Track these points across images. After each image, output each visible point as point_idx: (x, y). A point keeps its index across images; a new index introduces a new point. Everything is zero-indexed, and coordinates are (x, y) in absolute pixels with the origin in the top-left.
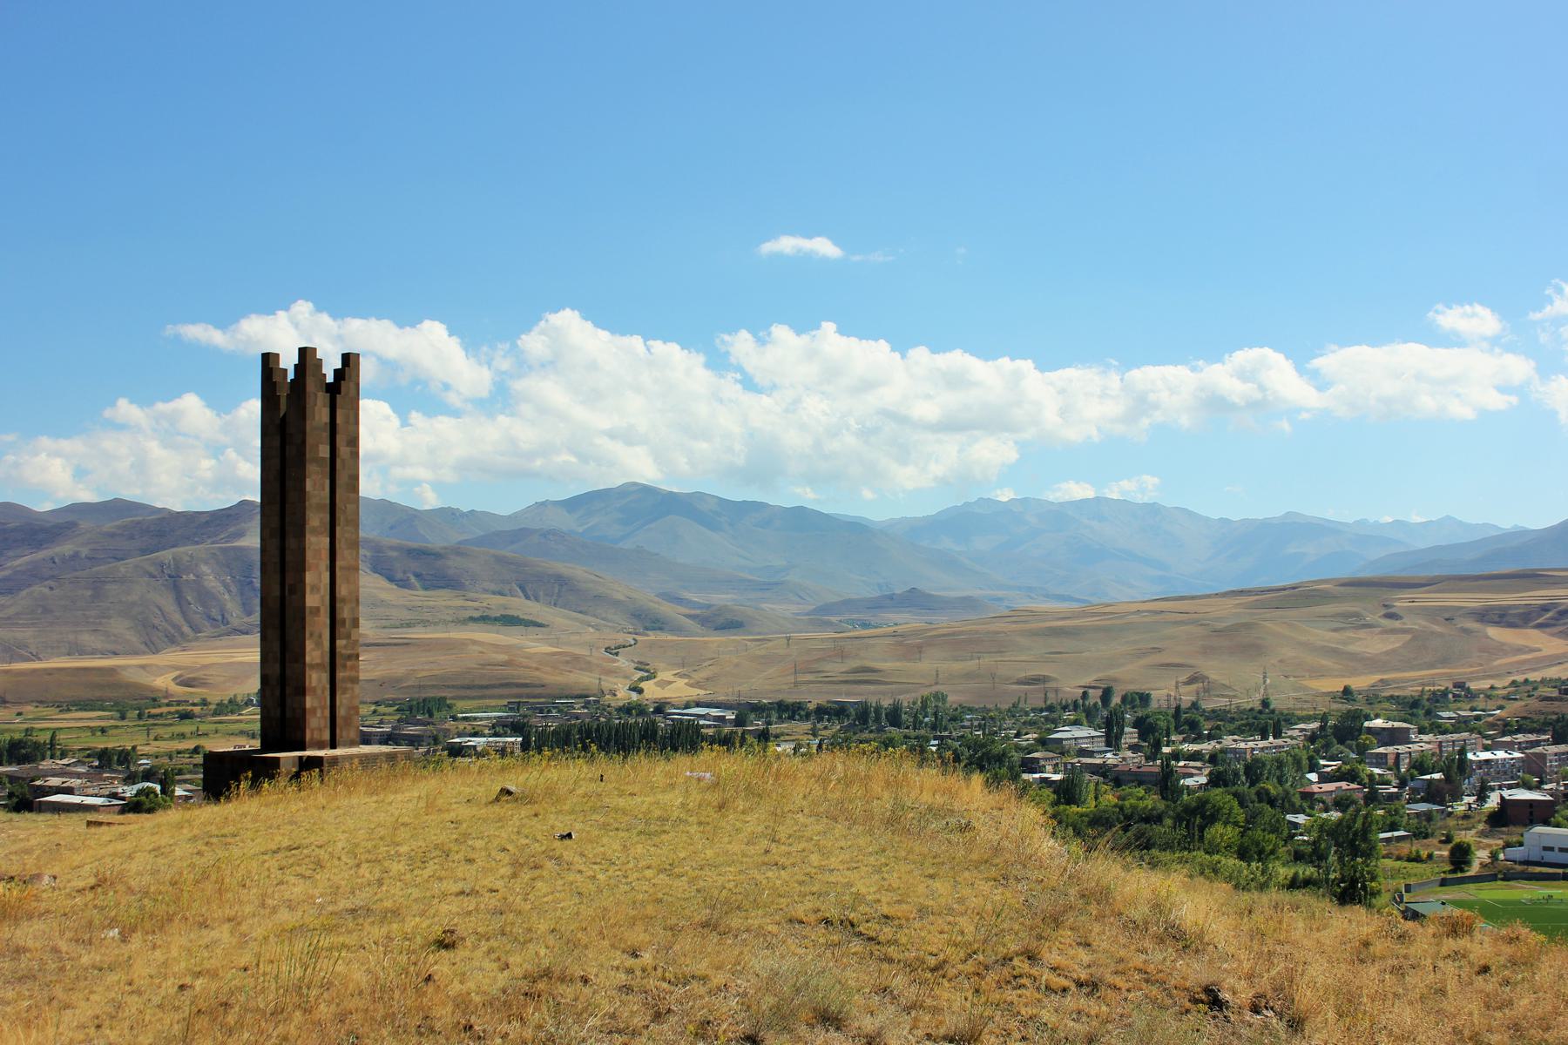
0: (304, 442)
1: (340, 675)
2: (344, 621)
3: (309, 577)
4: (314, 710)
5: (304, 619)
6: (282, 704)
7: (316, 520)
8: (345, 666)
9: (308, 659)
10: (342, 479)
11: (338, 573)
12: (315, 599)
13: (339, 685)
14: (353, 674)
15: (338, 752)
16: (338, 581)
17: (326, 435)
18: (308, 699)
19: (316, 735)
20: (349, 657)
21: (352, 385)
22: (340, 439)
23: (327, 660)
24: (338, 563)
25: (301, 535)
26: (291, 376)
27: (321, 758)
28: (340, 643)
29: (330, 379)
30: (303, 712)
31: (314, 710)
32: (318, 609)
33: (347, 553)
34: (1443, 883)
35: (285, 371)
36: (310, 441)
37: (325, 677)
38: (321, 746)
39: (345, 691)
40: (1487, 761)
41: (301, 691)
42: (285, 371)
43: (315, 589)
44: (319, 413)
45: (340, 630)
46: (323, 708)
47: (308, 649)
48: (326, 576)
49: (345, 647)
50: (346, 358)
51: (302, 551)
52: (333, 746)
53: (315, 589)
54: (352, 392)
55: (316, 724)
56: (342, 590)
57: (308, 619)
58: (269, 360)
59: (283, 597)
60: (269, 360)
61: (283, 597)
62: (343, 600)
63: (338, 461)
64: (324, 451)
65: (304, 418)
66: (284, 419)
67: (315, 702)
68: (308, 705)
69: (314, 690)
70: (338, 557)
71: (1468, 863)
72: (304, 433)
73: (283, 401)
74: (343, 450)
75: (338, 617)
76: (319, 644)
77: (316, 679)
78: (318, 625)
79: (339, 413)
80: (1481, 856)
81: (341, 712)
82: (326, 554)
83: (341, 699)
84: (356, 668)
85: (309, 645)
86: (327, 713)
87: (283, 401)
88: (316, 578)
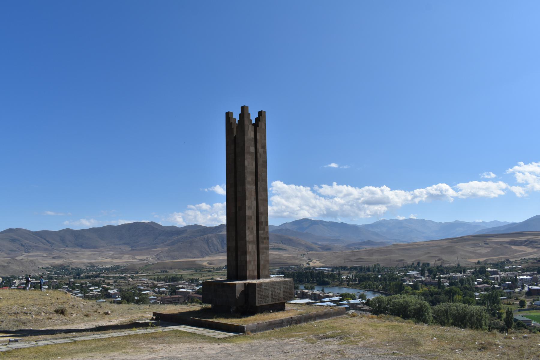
0: (244, 145)
1: (261, 246)
2: (262, 222)
3: (247, 203)
4: (250, 262)
5: (245, 221)
7: (250, 178)
8: (263, 242)
9: (247, 239)
10: (260, 161)
11: (259, 202)
12: (250, 212)
13: (260, 251)
14: (266, 246)
15: (262, 281)
16: (259, 205)
17: (253, 143)
18: (248, 257)
19: (251, 273)
20: (265, 238)
21: (263, 123)
23: (255, 239)
24: (260, 198)
25: (244, 184)
26: (238, 119)
27: (254, 284)
28: (261, 232)
29: (254, 122)
31: (250, 262)
34: (519, 311)
37: (255, 247)
38: (254, 279)
39: (263, 253)
41: (245, 253)
43: (250, 208)
44: (250, 134)
45: (261, 227)
47: (247, 234)
49: (263, 234)
50: (261, 113)
51: (244, 191)
53: (250, 208)
55: (251, 268)
56: (261, 209)
57: (247, 221)
58: (228, 116)
59: (236, 212)
60: (228, 116)
61: (236, 212)
62: (262, 214)
63: (258, 154)
64: (252, 149)
65: (244, 135)
67: (251, 258)
68: (248, 259)
69: (250, 252)
70: (259, 195)
71: (525, 305)
72: (244, 141)
73: (235, 130)
74: (260, 150)
76: (252, 232)
77: (251, 248)
78: (251, 224)
79: (258, 134)
80: (528, 303)
81: (262, 263)
82: (254, 194)
83: (262, 257)
84: (267, 243)
85: (248, 233)
87: (235, 130)
88: (250, 202)
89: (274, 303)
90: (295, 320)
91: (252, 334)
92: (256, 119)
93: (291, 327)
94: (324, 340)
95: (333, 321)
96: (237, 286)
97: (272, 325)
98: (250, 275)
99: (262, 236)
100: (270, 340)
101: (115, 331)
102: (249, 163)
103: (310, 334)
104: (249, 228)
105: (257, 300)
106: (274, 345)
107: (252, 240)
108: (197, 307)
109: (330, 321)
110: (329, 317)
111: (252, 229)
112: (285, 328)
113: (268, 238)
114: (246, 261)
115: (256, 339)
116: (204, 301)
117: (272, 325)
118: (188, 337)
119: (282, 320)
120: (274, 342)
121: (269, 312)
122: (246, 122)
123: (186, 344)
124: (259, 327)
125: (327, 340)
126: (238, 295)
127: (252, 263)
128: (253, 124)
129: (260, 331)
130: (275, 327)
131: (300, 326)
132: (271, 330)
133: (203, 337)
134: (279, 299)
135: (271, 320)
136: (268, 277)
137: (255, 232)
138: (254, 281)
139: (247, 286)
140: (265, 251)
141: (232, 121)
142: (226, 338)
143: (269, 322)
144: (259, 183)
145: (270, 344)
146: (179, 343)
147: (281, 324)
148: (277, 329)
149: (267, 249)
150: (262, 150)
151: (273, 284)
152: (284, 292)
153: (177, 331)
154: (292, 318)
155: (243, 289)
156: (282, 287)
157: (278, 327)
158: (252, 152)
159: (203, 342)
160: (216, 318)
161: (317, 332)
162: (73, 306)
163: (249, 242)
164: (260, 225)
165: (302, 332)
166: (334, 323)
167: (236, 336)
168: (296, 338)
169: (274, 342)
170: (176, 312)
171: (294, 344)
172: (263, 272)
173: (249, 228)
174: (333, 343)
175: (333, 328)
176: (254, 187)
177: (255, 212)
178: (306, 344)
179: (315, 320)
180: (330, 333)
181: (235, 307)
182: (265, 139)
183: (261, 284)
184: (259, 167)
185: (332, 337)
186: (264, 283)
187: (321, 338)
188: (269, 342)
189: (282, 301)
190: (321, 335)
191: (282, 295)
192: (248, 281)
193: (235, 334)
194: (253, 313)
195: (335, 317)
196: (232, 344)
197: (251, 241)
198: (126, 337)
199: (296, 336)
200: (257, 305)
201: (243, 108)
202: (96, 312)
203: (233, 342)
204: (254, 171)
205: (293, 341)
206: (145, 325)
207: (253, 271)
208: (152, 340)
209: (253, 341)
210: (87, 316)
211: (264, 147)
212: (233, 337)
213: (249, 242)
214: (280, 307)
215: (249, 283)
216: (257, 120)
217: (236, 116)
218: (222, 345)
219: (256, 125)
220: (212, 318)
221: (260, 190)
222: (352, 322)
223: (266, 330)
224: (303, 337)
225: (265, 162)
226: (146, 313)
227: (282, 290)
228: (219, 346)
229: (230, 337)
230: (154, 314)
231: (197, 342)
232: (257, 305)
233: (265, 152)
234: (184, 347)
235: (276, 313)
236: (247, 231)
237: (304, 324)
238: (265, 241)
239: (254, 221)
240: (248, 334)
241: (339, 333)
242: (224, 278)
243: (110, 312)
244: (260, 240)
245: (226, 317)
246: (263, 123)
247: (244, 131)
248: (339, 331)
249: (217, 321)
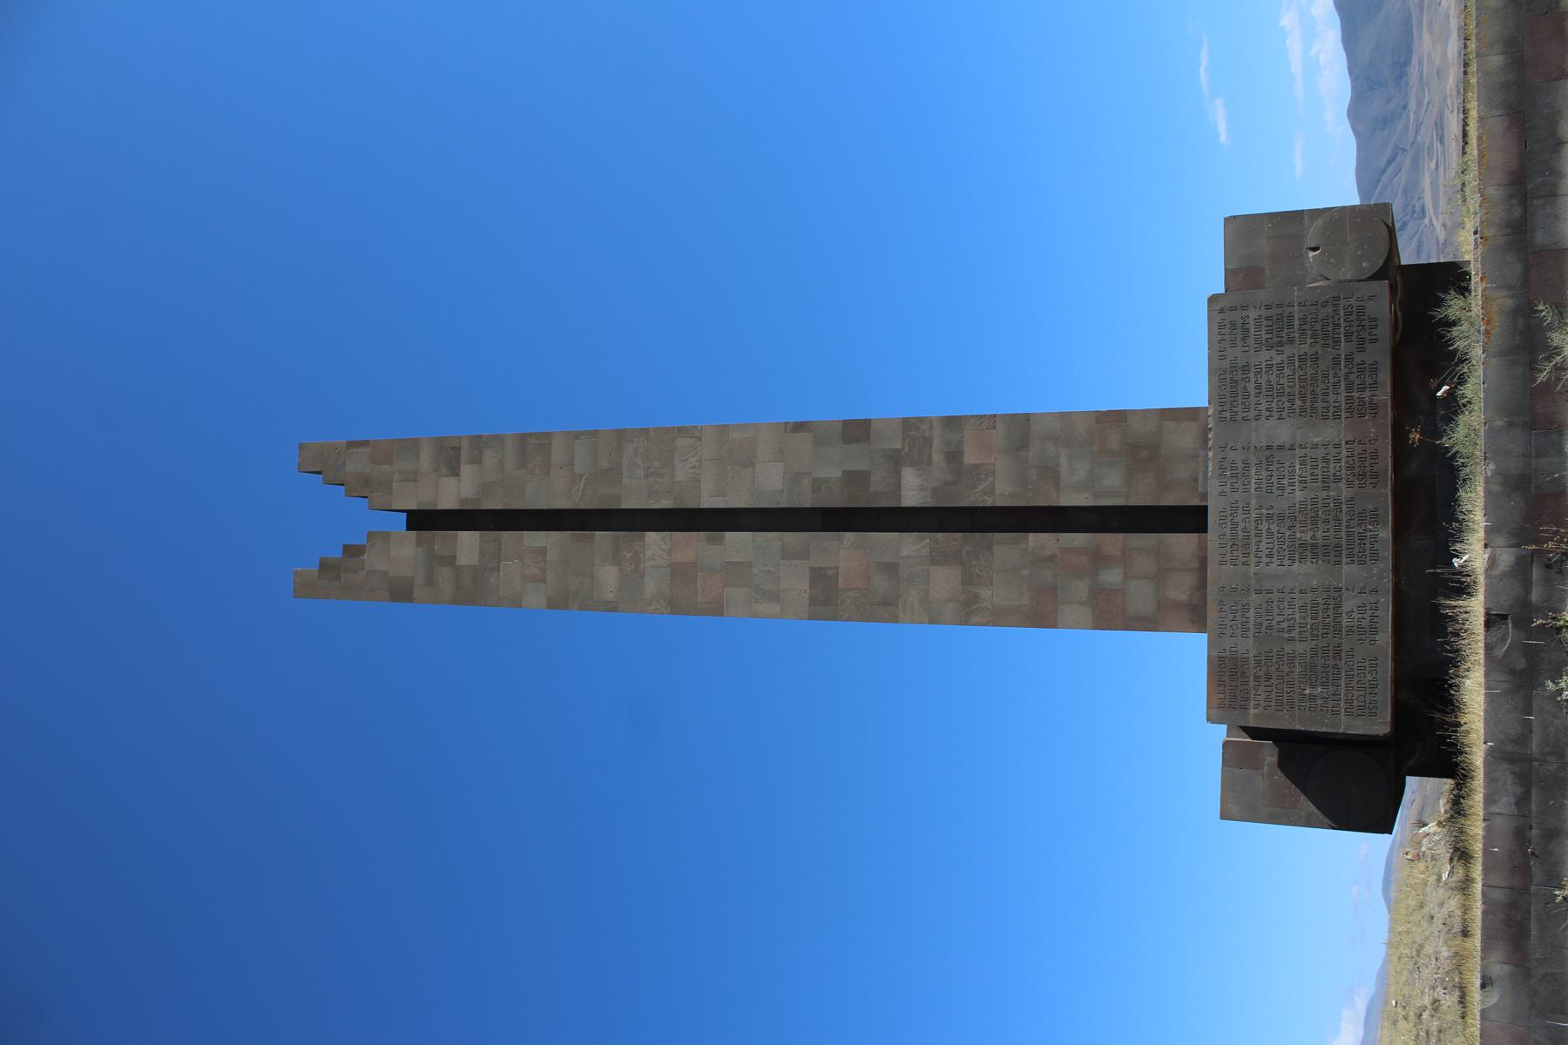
33: (682, 473)
39: (1050, 472)
46: (1098, 559)
86: (1111, 542)
89: (1385, 534)
127: (1112, 577)
137: (909, 546)
144: (628, 504)
150: (467, 470)
176: (654, 540)
191: (1332, 432)
197: (968, 580)
200: (1380, 725)
227: (1283, 432)
238: (970, 458)
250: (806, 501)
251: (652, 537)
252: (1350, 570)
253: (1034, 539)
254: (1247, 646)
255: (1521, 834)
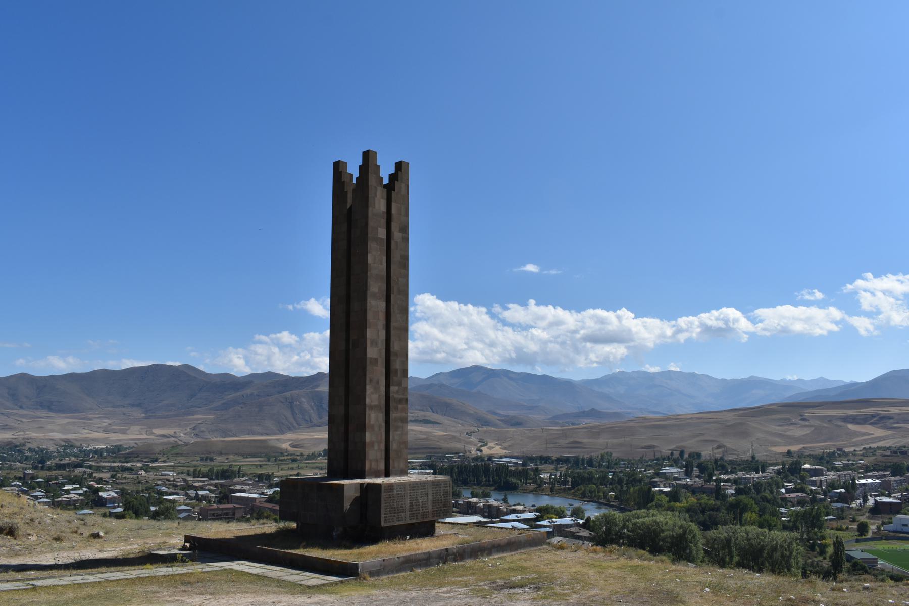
0: (367, 224)
1: (393, 415)
2: (396, 371)
3: (370, 334)
4: (372, 444)
6: (347, 440)
7: (375, 287)
8: (397, 408)
9: (368, 401)
10: (396, 256)
11: (392, 332)
12: (374, 352)
13: (392, 423)
14: (404, 414)
15: (392, 480)
16: (392, 338)
17: (383, 221)
19: (374, 465)
21: (403, 185)
22: (395, 227)
23: (383, 402)
24: (393, 324)
25: (364, 299)
26: (356, 174)
27: (379, 486)
28: (393, 389)
29: (386, 181)
30: (362, 447)
31: (372, 444)
32: (376, 360)
34: (857, 541)
35: (352, 175)
36: (371, 223)
37: (381, 416)
38: (377, 476)
40: (864, 484)
41: (362, 428)
42: (352, 175)
43: (374, 343)
44: (379, 204)
45: (394, 379)
47: (368, 392)
48: (383, 334)
49: (397, 392)
50: (399, 166)
51: (365, 312)
52: (387, 475)
53: (374, 343)
54: (403, 192)
55: (374, 456)
56: (395, 347)
57: (368, 367)
58: (339, 167)
59: (347, 351)
60: (339, 167)
61: (347, 351)
62: (396, 354)
64: (382, 233)
65: (367, 206)
66: (351, 207)
67: (373, 437)
70: (393, 319)
71: (867, 532)
73: (350, 196)
74: (397, 235)
75: (392, 367)
77: (374, 418)
78: (376, 373)
79: (394, 205)
80: (873, 528)
81: (394, 446)
84: (405, 410)
85: (369, 389)
86: (383, 447)
87: (350, 196)
88: (375, 333)
89: (414, 521)
90: (454, 554)
91: (373, 579)
92: (390, 176)
93: (446, 567)
94: (506, 591)
95: (524, 556)
96: (346, 488)
97: (410, 563)
98: (370, 468)
99: (396, 396)
100: (405, 590)
101: (112, 569)
102: (375, 259)
103: (481, 581)
104: (371, 381)
105: (383, 516)
106: (412, 599)
107: (376, 403)
108: (270, 527)
109: (518, 557)
110: (516, 550)
111: (378, 383)
112: (433, 569)
113: (407, 400)
114: (364, 443)
115: (380, 589)
116: (284, 517)
117: (410, 563)
118: (251, 582)
119: (429, 553)
120: (414, 594)
121: (404, 539)
122: (372, 181)
123: (246, 595)
124: (385, 566)
125: (512, 591)
126: (347, 505)
127: (376, 447)
128: (385, 186)
129: (388, 573)
130: (415, 567)
131: (462, 566)
132: (408, 573)
133: (281, 584)
134: (424, 515)
135: (408, 554)
136: (404, 473)
137: (383, 389)
138: (379, 481)
139: (366, 489)
140: (400, 424)
141: (345, 179)
142: (324, 585)
143: (404, 557)
144: (392, 296)
145: (405, 597)
146: (234, 593)
147: (426, 560)
148: (418, 571)
149: (405, 420)
150: (401, 235)
151: (414, 485)
152: (434, 502)
153: (231, 571)
154: (447, 550)
155: (358, 495)
156: (430, 492)
157: (420, 566)
158: (382, 239)
159: (280, 593)
160: (305, 548)
161: (494, 577)
162: (32, 520)
163: (372, 407)
164: (392, 375)
165: (466, 576)
166: (525, 560)
167: (342, 582)
168: (454, 588)
169: (414, 594)
170: (229, 536)
171: (450, 598)
172: (396, 465)
173: (371, 381)
174: (522, 598)
175: (522, 569)
177: (384, 351)
178: (472, 598)
179: (490, 554)
180: (517, 578)
181: (341, 529)
182: (407, 215)
183: (391, 486)
184: (393, 267)
185: (521, 587)
186: (398, 484)
187: (500, 588)
188: (403, 594)
189: (430, 519)
190: (501, 582)
191: (430, 507)
192: (367, 480)
193: (340, 579)
194: (374, 541)
195: (527, 550)
196: (334, 596)
197: (376, 406)
198: (132, 581)
199: (454, 583)
200: (383, 524)
201: (368, 156)
202: (76, 532)
203: (336, 594)
204: (384, 273)
205: (448, 592)
206: (169, 559)
207: (377, 461)
208: (183, 588)
209: (374, 592)
210: (57, 539)
211: (405, 229)
212: (336, 583)
213: (372, 407)
214: (426, 530)
215: (368, 484)
216: (393, 177)
217: (353, 170)
218: (317, 598)
219: (390, 188)
220: (298, 548)
221: (394, 310)
222: (557, 558)
223: (397, 572)
224: (466, 586)
225: (405, 258)
226: (171, 537)
227: (430, 497)
228: (309, 601)
229: (332, 584)
230: (188, 539)
231: (268, 592)
232: (383, 524)
233: (406, 240)
234: (244, 600)
235: (419, 541)
236: (368, 387)
237: (469, 562)
238: (400, 406)
239: (381, 369)
240: (365, 579)
241: (533, 579)
242: (322, 473)
243: (102, 534)
244: (392, 404)
245: (324, 547)
246: (403, 185)
247: (367, 197)
248: (534, 575)
249: (307, 554)
250: (392, 358)
251: (384, 304)
252: (408, 513)
253: (384, 424)
254: (395, 492)
255: (419, 560)
